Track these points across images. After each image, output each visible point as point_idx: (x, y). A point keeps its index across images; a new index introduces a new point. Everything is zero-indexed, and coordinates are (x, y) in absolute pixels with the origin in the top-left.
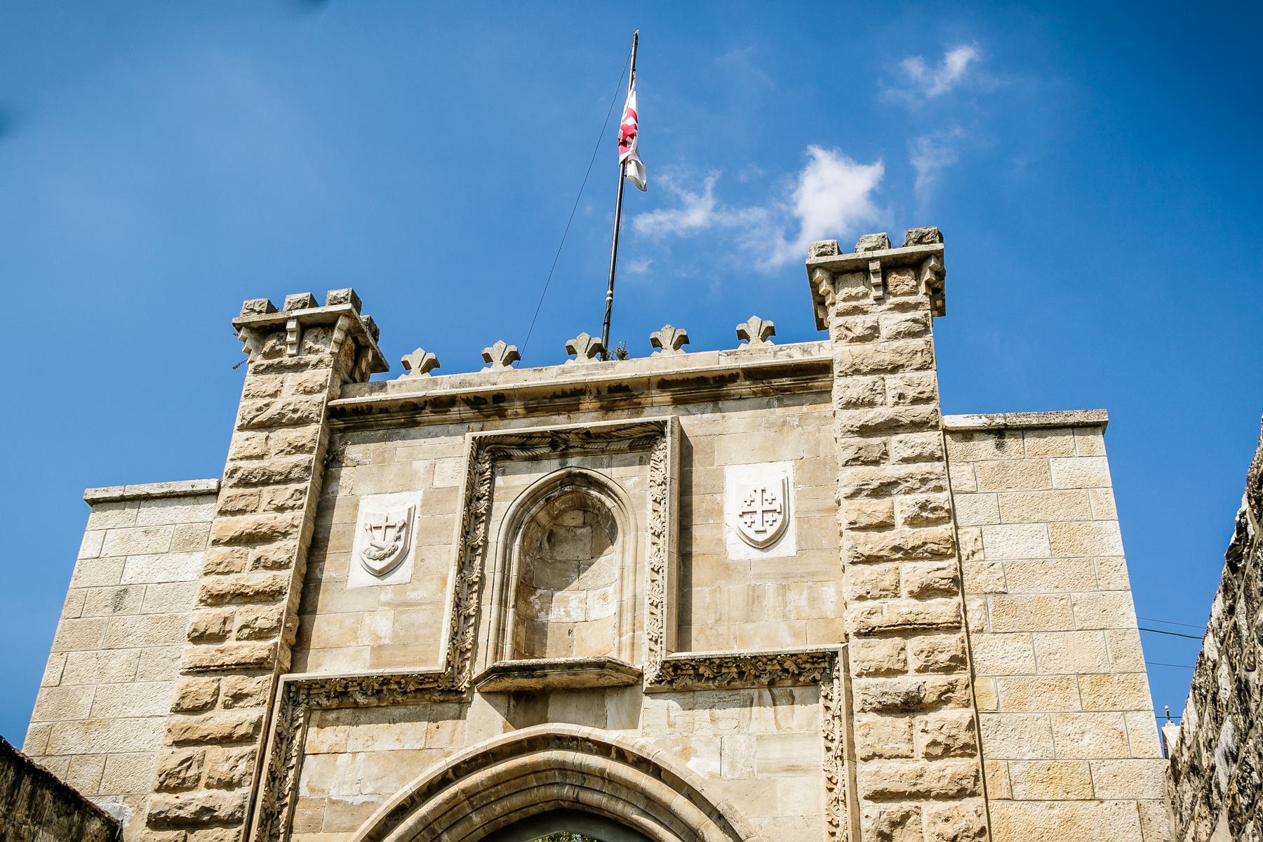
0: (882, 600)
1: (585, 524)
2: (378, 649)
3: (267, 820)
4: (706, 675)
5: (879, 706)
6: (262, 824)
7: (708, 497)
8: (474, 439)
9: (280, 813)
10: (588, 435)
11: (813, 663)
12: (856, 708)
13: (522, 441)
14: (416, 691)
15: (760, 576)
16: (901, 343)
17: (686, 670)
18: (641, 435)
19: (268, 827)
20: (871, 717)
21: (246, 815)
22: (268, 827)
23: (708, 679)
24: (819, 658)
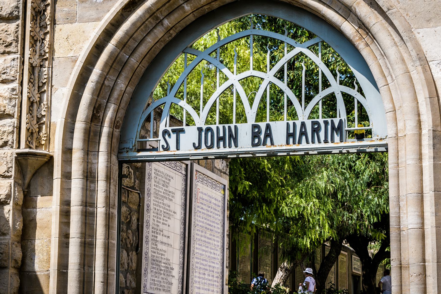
3: (37, 16)
6: (34, 19)
9: (45, 11)
19: (38, 21)
21: (21, 13)
22: (38, 21)
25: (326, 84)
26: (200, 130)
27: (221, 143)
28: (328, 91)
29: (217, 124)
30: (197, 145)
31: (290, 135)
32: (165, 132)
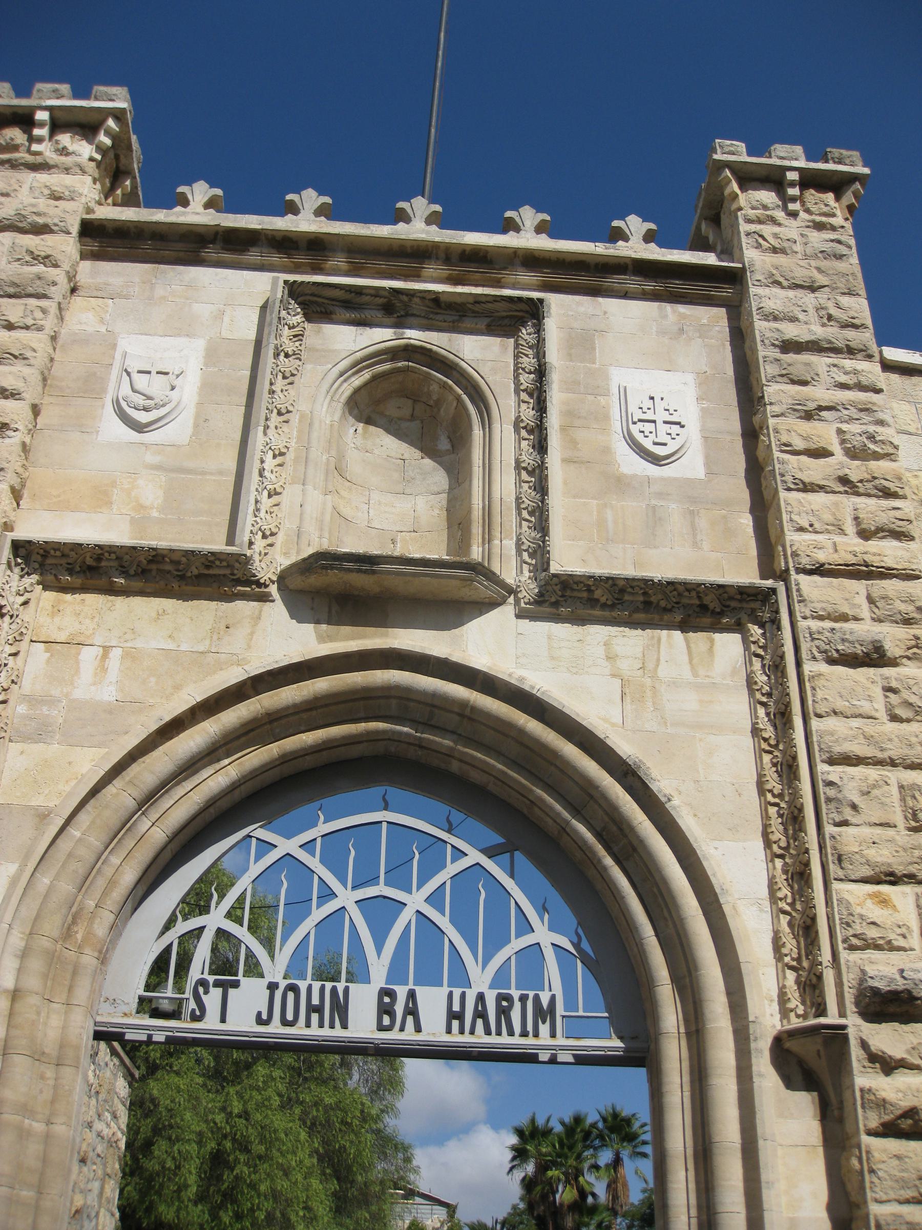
0: (827, 536)
1: (413, 417)
2: (137, 523)
4: (603, 600)
5: (835, 655)
7: (590, 398)
8: (286, 282)
10: (436, 300)
11: (740, 601)
12: (804, 655)
13: (348, 296)
14: (199, 576)
15: (660, 495)
16: (824, 264)
17: (579, 591)
18: (505, 314)
20: (824, 667)
23: (604, 606)
24: (749, 595)
25: (526, 927)
26: (272, 987)
27: (315, 1017)
28: (528, 940)
29: (309, 981)
30: (264, 1016)
31: (454, 1016)
32: (203, 983)
